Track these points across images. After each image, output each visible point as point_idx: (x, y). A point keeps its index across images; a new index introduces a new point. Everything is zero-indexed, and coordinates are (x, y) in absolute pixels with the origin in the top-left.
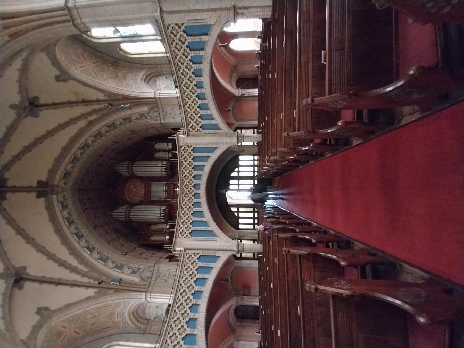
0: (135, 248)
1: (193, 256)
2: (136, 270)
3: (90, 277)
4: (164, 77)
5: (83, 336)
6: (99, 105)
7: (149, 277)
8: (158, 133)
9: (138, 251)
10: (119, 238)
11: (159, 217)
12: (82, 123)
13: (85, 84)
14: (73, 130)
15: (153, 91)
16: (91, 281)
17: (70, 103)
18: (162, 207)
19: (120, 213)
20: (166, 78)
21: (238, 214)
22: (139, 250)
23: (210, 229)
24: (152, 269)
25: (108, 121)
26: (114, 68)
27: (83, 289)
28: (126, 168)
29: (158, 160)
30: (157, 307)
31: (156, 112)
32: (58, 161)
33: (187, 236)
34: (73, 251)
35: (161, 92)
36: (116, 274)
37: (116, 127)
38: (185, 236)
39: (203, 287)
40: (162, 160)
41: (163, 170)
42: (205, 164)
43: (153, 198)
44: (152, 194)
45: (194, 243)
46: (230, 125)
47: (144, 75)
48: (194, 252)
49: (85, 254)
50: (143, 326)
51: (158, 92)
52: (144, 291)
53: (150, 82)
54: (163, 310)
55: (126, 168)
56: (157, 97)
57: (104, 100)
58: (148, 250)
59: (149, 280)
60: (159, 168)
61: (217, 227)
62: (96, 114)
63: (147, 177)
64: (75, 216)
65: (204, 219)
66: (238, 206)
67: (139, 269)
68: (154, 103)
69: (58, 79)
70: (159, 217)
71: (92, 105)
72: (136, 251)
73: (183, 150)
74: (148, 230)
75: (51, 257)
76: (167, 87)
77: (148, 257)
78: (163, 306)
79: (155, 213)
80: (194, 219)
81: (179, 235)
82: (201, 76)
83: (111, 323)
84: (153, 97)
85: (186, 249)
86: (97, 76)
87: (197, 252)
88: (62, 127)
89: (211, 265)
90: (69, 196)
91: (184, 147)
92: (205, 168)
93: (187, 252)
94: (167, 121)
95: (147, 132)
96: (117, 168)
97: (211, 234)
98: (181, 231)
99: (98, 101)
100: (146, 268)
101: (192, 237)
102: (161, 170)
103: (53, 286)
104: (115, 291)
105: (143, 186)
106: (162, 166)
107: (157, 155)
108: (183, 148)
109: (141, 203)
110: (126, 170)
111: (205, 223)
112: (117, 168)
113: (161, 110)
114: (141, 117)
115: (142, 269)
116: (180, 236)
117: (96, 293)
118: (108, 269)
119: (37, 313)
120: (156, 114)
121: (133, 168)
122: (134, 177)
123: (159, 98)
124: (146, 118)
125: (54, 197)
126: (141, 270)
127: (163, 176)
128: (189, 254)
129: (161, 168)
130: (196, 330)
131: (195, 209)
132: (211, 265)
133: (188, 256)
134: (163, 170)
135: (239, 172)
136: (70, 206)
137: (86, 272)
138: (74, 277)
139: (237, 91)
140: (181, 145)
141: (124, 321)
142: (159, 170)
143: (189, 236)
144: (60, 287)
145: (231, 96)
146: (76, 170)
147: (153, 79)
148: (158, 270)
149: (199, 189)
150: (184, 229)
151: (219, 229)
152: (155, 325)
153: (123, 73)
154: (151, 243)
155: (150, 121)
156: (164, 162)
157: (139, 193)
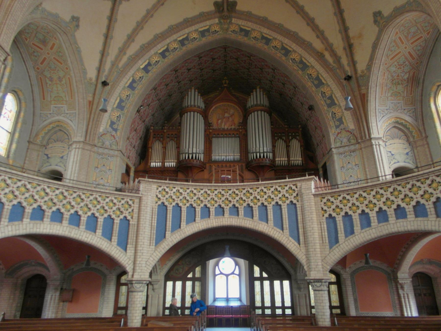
0: (144, 121)
1: (130, 210)
2: (115, 126)
3: (110, 71)
4: (407, 151)
5: (38, 69)
6: (349, 65)
7: (103, 143)
8: (316, 144)
9: (140, 126)
10: (159, 100)
12: (318, 45)
13: (375, 46)
14: (308, 34)
15: (381, 135)
16: (106, 73)
17: (345, 30)
19: (194, 99)
20: (407, 154)
21: (189, 279)
22: (141, 128)
23: (168, 234)
24: (114, 147)
25: (325, 76)
26: (408, 78)
27: (96, 64)
28: (259, 103)
29: (274, 146)
30: (62, 157)
31: (349, 140)
32: (264, 21)
33: (159, 199)
34: (145, 48)
35: (382, 148)
36: (113, 101)
37: (317, 86)
38: (160, 196)
39: (84, 227)
40: (274, 152)
41: (258, 155)
42: (271, 222)
43: (214, 140)
44: (221, 140)
45: (149, 210)
46: (343, 262)
47: (405, 120)
48: (136, 210)
49: (140, 62)
50: (38, 141)
51: (381, 142)
52: (85, 140)
53: (396, 130)
54: (57, 165)
55: (259, 103)
56: (373, 142)
57: (355, 70)
59: (100, 144)
61: (171, 245)
62: (334, 62)
63: (246, 131)
64: (190, 46)
65: (183, 224)
66: (203, 280)
67: (116, 130)
68: (362, 138)
69: (377, 15)
70: (187, 151)
71: (347, 55)
72: (140, 122)
73: (290, 188)
74: (168, 137)
75: (140, 26)
76: (393, 155)
77: (131, 140)
78: (62, 165)
79: (194, 145)
80: (184, 209)
81: (160, 186)
82: (416, 216)
83: (49, 100)
84: (372, 136)
85: (140, 198)
86: (391, 59)
87: (135, 215)
88: (311, 22)
89: (115, 238)
90: (217, 37)
91: (296, 189)
92: (264, 223)
93: (137, 201)
94: (336, 157)
95: (316, 128)
96: (258, 90)
97: (161, 235)
98: (167, 190)
99: (353, 63)
100: (117, 139)
101: (157, 207)
102: (258, 150)
103: (104, 30)
104: (90, 102)
105: (233, 127)
106: (264, 152)
107: (281, 144)
108: (294, 187)
109: (208, 125)
110: (255, 103)
111: (177, 226)
112: (258, 90)
113: (352, 148)
114: (338, 120)
115: (115, 135)
116: (160, 189)
117: (91, 79)
118: (119, 91)
119: (73, 18)
120: (345, 140)
121: (259, 112)
122: (246, 113)
123: (372, 145)
124: (337, 127)
125: (217, 20)
126: (114, 133)
127: (250, 155)
128: (133, 203)
129: (262, 151)
130: (28, 220)
131: (198, 210)
132: (115, 238)
133: (130, 202)
134: (258, 155)
135: (261, 279)
136: (204, 39)
137: (118, 66)
138: (113, 52)
139: (406, 275)
140: (299, 184)
141: (49, 116)
142: (258, 149)
143: (160, 203)
144: (102, 39)
145: (395, 264)
146: (252, 42)
147: (402, 134)
148: (112, 156)
149: (231, 214)
150: (169, 195)
151: (167, 248)
152: (38, 156)
153: (403, 92)
154: (150, 142)
155: (332, 133)
156: (271, 155)
157: (222, 122)
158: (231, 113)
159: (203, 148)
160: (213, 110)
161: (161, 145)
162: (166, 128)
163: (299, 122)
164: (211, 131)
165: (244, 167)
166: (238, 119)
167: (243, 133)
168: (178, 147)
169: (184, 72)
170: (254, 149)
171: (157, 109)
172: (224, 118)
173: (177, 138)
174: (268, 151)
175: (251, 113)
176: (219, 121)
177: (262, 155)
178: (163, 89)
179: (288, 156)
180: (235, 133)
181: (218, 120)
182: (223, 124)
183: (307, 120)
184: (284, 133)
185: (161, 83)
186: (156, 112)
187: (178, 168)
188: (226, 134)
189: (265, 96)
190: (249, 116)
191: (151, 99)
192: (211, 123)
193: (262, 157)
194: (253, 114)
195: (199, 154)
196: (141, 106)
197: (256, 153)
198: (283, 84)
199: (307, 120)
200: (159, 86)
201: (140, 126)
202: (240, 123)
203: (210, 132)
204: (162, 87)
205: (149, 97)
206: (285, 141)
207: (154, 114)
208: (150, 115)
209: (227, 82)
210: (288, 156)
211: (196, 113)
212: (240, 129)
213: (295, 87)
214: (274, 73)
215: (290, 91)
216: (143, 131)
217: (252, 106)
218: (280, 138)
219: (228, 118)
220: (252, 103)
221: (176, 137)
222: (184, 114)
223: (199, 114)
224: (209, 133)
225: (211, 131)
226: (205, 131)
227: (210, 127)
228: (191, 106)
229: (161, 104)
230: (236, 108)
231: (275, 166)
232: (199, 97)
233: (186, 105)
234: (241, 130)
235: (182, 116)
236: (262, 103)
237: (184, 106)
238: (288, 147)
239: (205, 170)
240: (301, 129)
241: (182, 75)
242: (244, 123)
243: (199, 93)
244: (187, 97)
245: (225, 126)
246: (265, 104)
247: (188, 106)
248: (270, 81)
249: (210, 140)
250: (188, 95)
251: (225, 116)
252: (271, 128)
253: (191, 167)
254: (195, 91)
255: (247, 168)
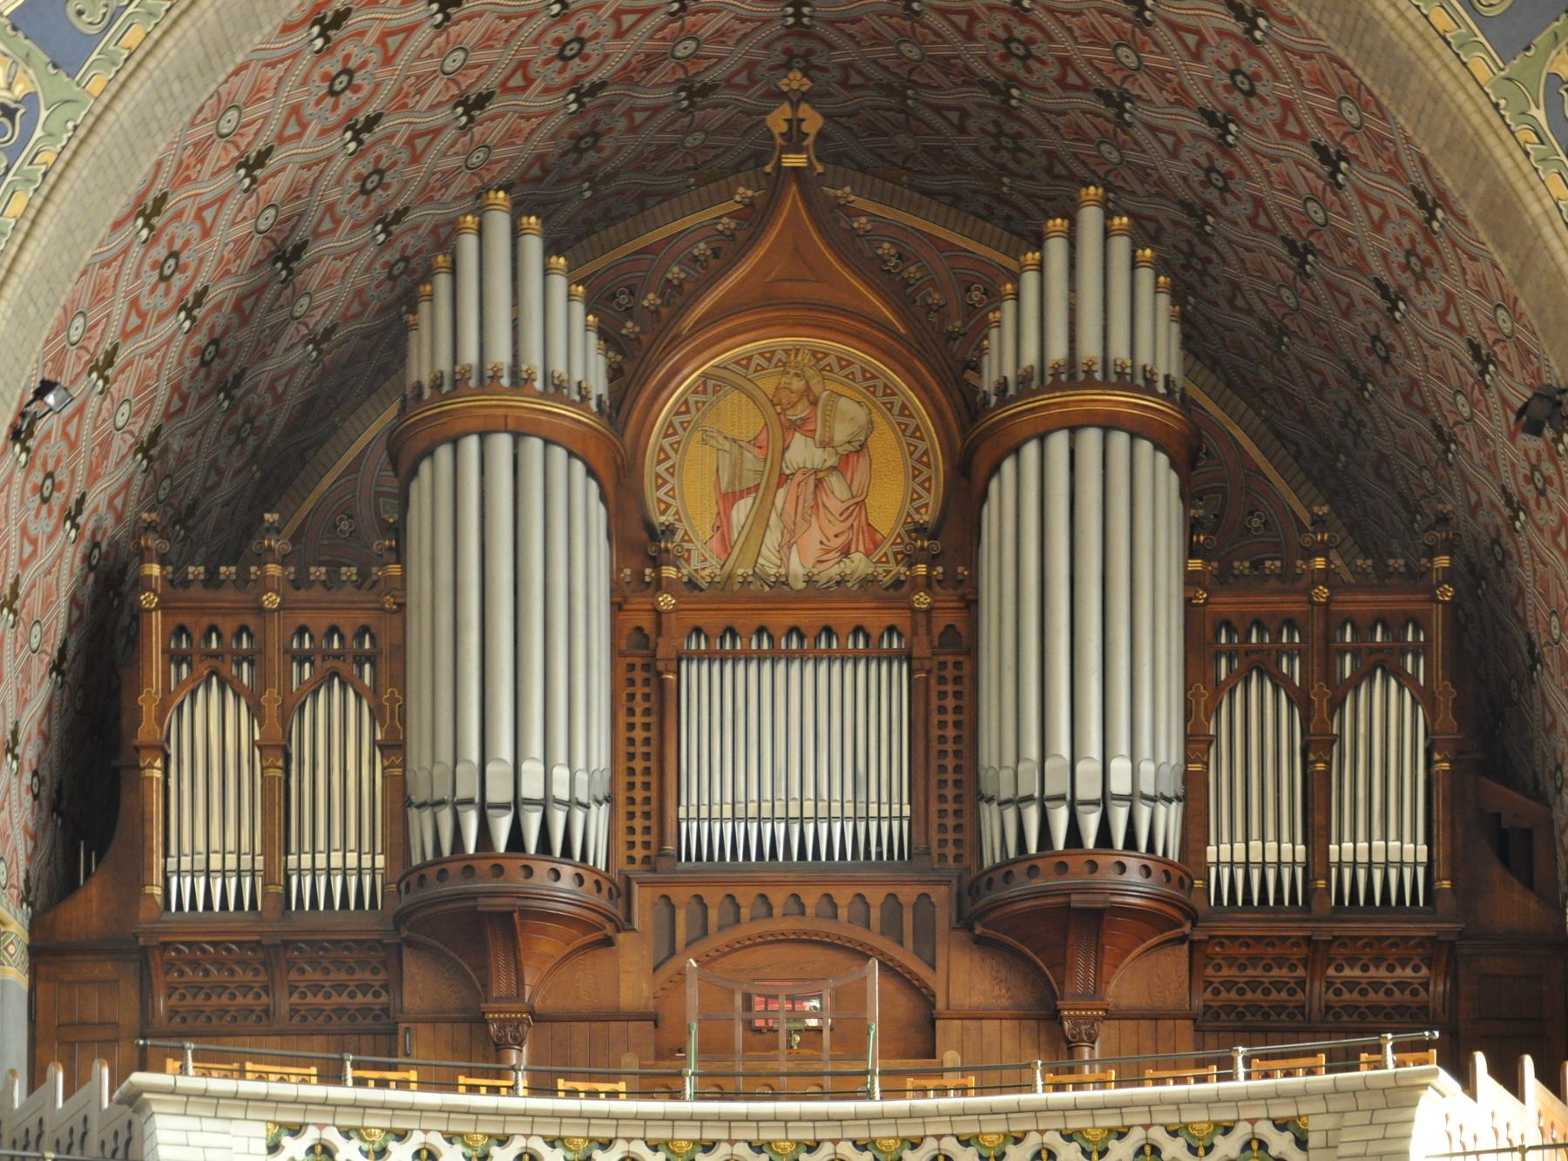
9: (46, 555)
11: (467, 787)
18: (600, 817)
19: (519, 312)
28: (1090, 348)
40: (1193, 795)
41: (1060, 819)
43: (699, 685)
58: (56, 667)
60: (1089, 768)
63: (971, 605)
72: (42, 526)
74: (302, 658)
96: (1091, 218)
105: (859, 564)
106: (1105, 800)
107: (1262, 718)
109: (640, 543)
112: (1091, 218)
121: (1091, 439)
122: (974, 439)
127: (990, 816)
134: (1060, 819)
156: (1169, 819)
157: (760, 520)
158: (841, 433)
159: (601, 757)
160: (683, 408)
161: (238, 716)
162: (273, 569)
163: (1443, 520)
164: (666, 601)
165: (944, 916)
166: (894, 496)
167: (941, 621)
168: (393, 747)
169: (410, 30)
170: (1029, 769)
171: (176, 388)
172: (783, 479)
173: (377, 657)
174: (1147, 788)
175: (1016, 451)
176: (742, 510)
177: (1091, 823)
178: (222, 199)
179: (1316, 832)
180: (876, 621)
181: (729, 499)
182: (773, 538)
183: (1515, 506)
184: (1291, 624)
185: (201, 150)
186: (168, 415)
187: (400, 919)
188: (794, 629)
189: (1145, 276)
190: (996, 469)
191: (119, 308)
192: (670, 530)
193: (1090, 842)
194: (1031, 451)
195: (571, 804)
196: (45, 387)
197: (1044, 803)
198: (1320, 150)
199: (1515, 506)
200: (183, 176)
201: (46, 555)
202: (920, 530)
203: (658, 613)
204: (210, 189)
205: (98, 296)
206: (1300, 699)
207: (154, 436)
208: (121, 444)
209: (813, 122)
210: (1316, 832)
211: (535, 445)
212: (914, 584)
213: (1430, 201)
214: (1251, 45)
215: (1378, 227)
216: (74, 600)
217: (1024, 380)
218: (1264, 665)
219: (819, 483)
220: (1030, 356)
221: (371, 658)
222: (430, 453)
223: (559, 454)
224: (646, 622)
225: (666, 601)
226: (617, 606)
227: (656, 563)
228: (487, 379)
229: (214, 342)
230: (889, 391)
231: (1192, 916)
232: (559, 283)
233: (444, 364)
234: (922, 600)
235: (414, 472)
236: (1120, 351)
237: (426, 380)
238: (1318, 746)
239: (621, 938)
240: (1447, 593)
241: (388, 60)
242: (950, 541)
243: (552, 247)
244: (443, 281)
245: (799, 551)
246: (1144, 357)
247: (458, 381)
248: (1188, 208)
249: (662, 684)
250: (454, 270)
251: (787, 460)
252: (1191, 580)
253: (505, 918)
254: (516, 233)
255: (963, 923)
